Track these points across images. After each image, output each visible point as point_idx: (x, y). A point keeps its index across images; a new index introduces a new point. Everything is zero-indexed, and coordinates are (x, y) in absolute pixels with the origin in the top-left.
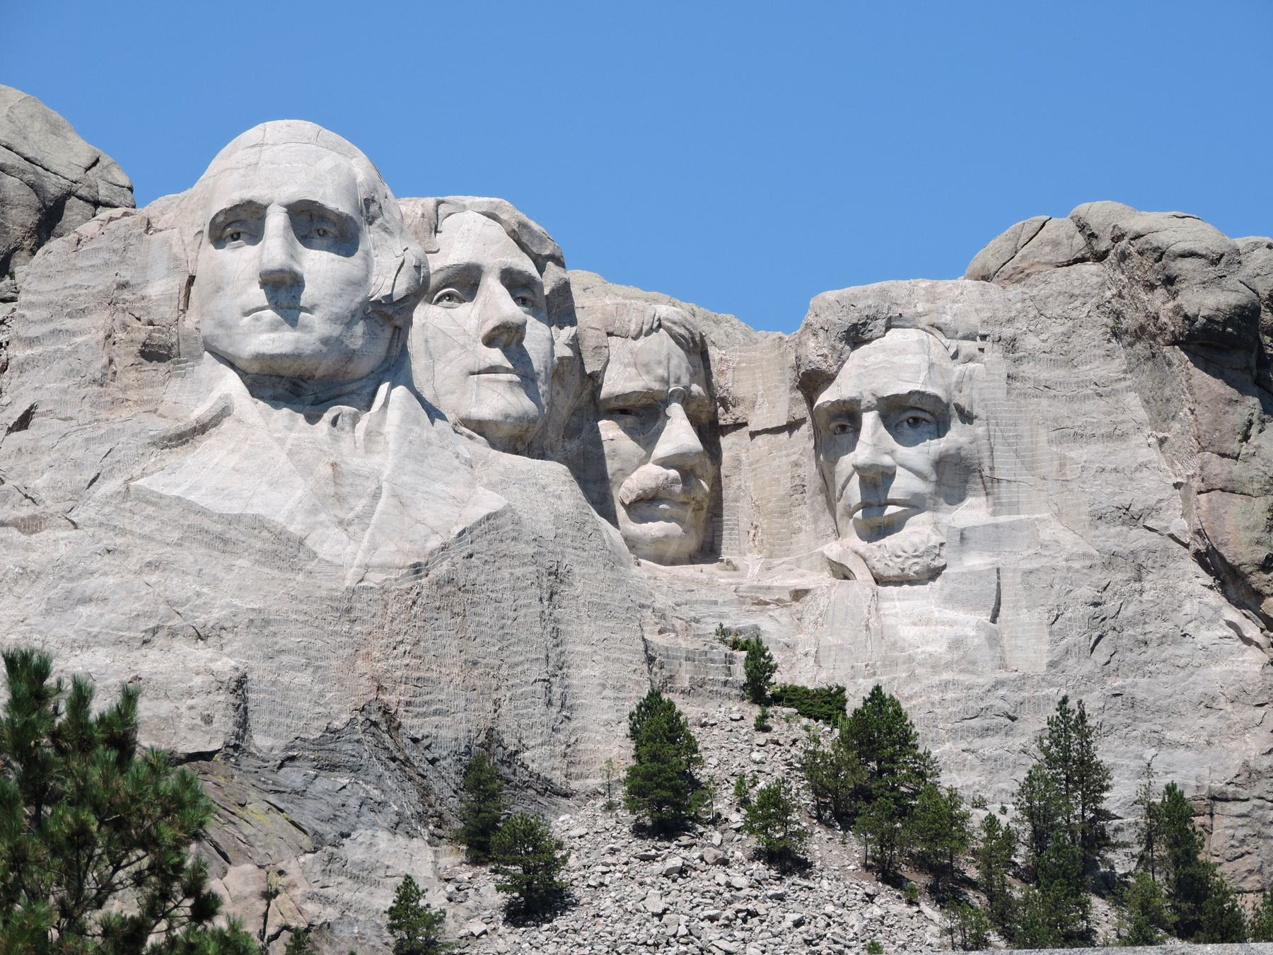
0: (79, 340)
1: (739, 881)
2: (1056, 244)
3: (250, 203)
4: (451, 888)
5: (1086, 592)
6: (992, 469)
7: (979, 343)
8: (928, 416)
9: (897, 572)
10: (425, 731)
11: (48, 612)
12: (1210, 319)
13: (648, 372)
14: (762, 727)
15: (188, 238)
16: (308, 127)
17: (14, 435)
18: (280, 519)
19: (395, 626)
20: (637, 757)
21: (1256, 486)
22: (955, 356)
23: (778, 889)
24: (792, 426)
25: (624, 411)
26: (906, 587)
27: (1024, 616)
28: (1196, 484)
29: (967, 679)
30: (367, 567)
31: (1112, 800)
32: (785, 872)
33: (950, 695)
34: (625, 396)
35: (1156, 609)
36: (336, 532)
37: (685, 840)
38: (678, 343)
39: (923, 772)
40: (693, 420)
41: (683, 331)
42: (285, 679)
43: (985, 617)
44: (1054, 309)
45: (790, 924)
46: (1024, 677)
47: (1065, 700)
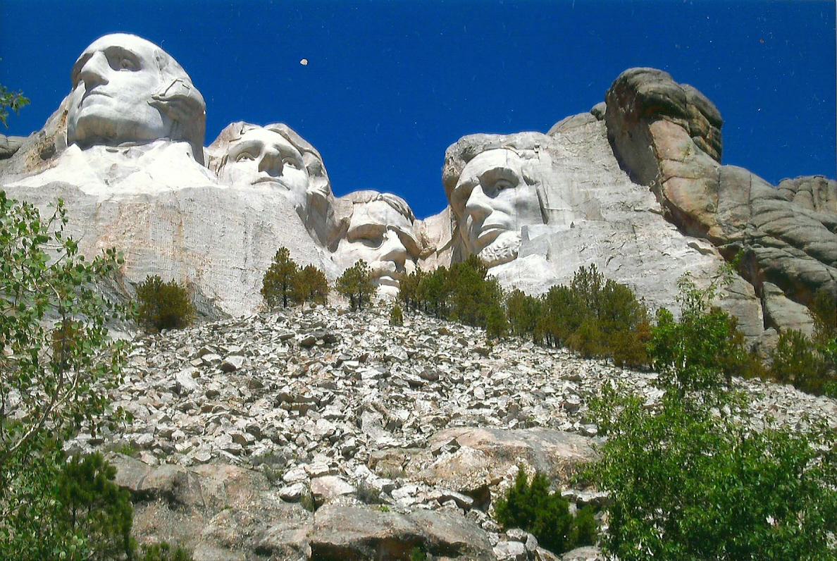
5: (601, 236)
6: (548, 205)
7: (536, 150)
8: (508, 184)
12: (654, 92)
13: (375, 217)
19: (127, 222)
21: (696, 173)
22: (524, 155)
29: (529, 280)
35: (646, 244)
41: (395, 202)
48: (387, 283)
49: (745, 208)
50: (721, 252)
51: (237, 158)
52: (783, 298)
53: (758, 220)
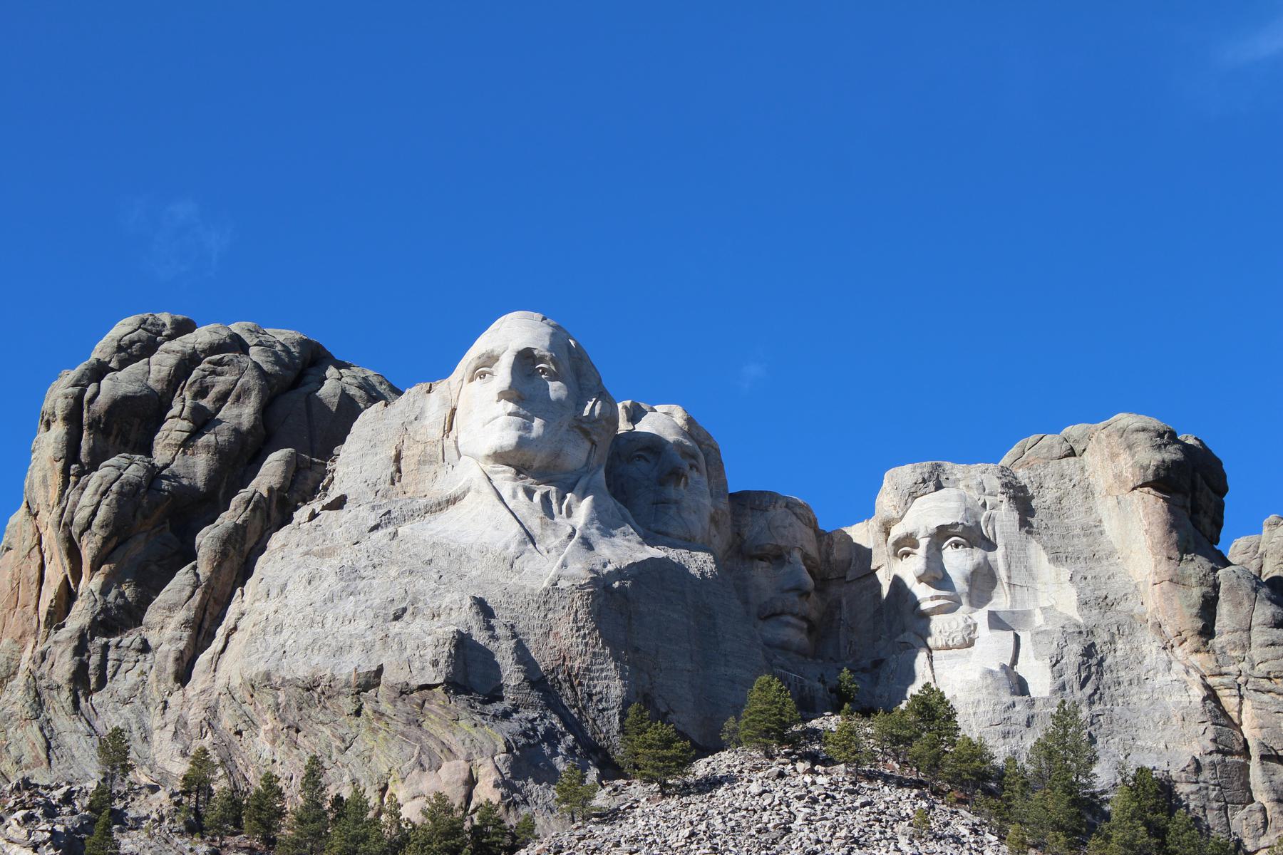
2: (1051, 447)
5: (1076, 648)
7: (1000, 497)
10: (598, 689)
16: (538, 316)
22: (984, 505)
25: (761, 559)
27: (1033, 662)
33: (981, 709)
38: (798, 518)
43: (1008, 663)
44: (1049, 483)
45: (857, 804)
48: (788, 624)
49: (1245, 636)
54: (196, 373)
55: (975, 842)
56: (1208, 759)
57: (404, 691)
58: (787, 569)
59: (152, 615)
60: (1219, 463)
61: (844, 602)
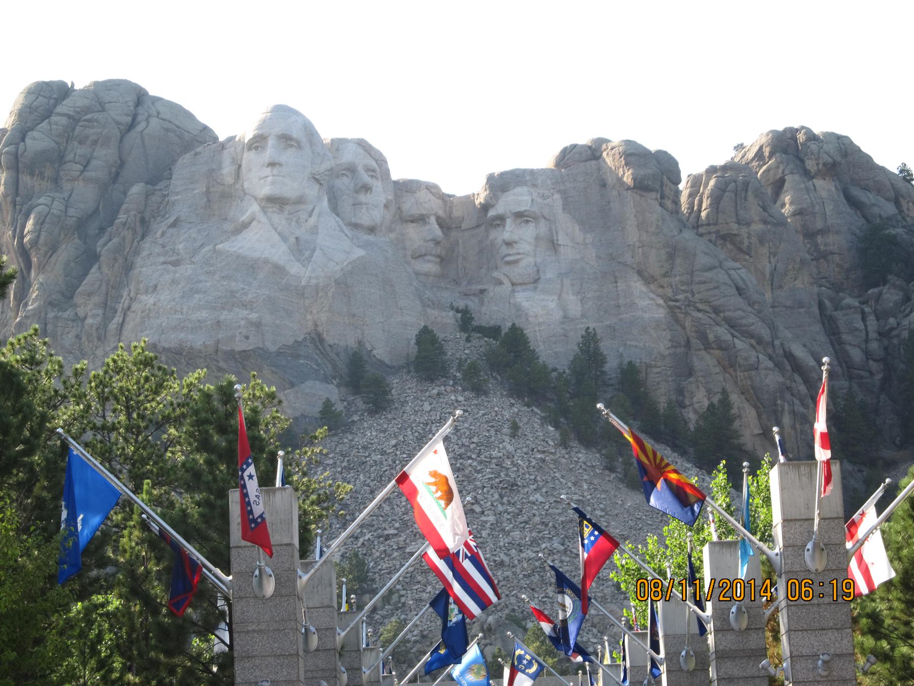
0: (195, 192)
1: (461, 398)
2: (581, 153)
3: (262, 135)
4: (345, 403)
9: (521, 281)
11: (183, 297)
14: (468, 340)
15: (239, 150)
17: (171, 230)
18: (275, 259)
20: (419, 352)
23: (475, 402)
24: (478, 226)
25: (412, 222)
26: (524, 287)
27: (571, 297)
28: (637, 244)
30: (310, 278)
31: (607, 367)
32: (478, 395)
34: (412, 216)
36: (297, 264)
37: (438, 383)
39: (533, 356)
40: (441, 226)
42: (278, 322)
43: (556, 297)
46: (572, 320)
47: (588, 328)
48: (429, 261)
50: (670, 307)
51: (337, 177)
52: (703, 353)
53: (695, 288)
54: (78, 129)
55: (544, 435)
56: (667, 352)
57: (231, 355)
58: (428, 227)
59: (78, 299)
60: (676, 163)
61: (460, 242)
